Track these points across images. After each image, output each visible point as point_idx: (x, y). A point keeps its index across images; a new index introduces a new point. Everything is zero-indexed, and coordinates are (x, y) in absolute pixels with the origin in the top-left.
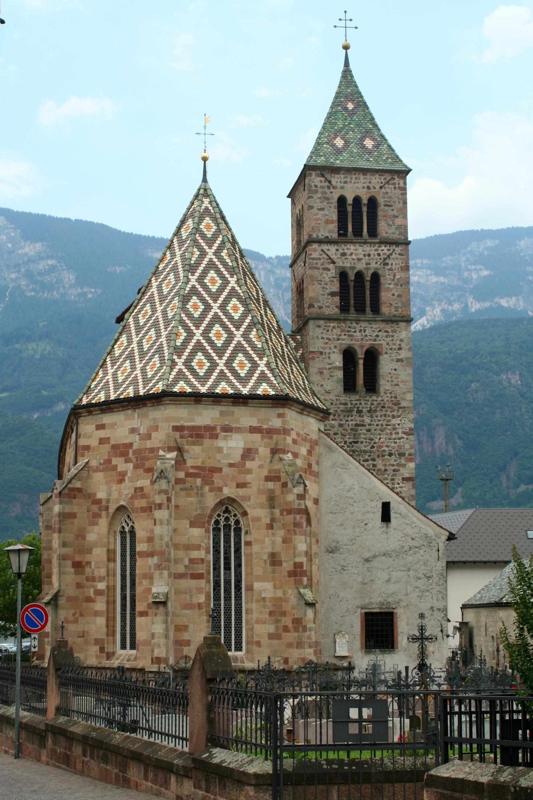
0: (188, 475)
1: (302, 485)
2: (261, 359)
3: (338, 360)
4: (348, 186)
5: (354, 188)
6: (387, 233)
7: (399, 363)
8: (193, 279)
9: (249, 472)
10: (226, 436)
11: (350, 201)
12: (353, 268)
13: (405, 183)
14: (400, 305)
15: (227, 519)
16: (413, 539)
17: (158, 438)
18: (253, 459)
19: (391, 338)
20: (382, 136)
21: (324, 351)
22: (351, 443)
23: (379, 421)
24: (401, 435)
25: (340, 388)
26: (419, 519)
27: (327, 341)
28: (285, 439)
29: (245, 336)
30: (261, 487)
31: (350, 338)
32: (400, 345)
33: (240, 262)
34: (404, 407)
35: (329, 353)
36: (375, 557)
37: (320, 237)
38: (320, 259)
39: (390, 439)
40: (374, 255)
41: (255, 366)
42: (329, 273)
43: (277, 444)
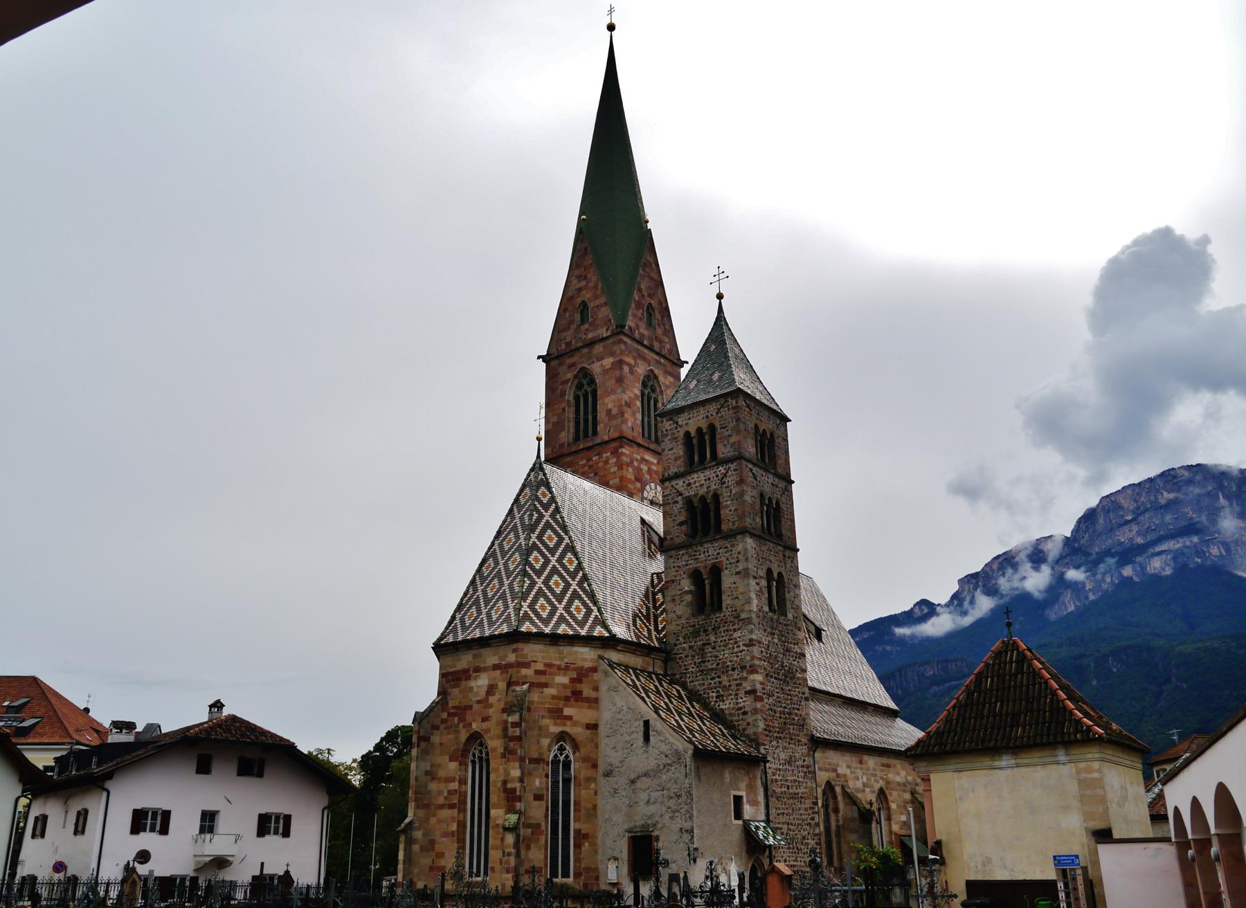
0: (450, 715)
3: (686, 585)
9: (491, 706)
12: (696, 495)
15: (481, 752)
24: (742, 648)
36: (638, 778)
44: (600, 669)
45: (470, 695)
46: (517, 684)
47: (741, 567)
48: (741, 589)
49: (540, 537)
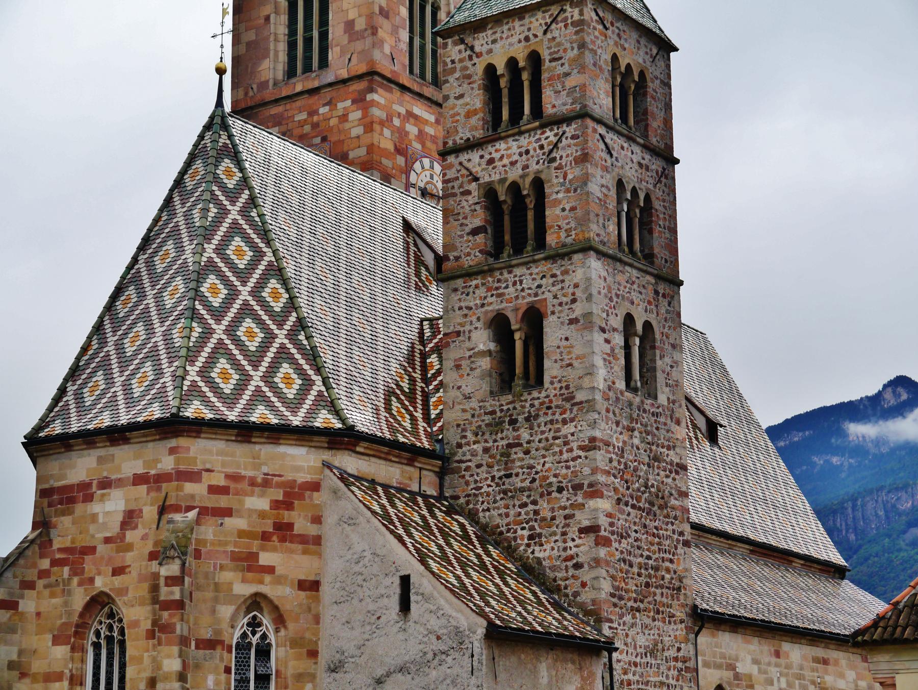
0: (54, 563)
1: (178, 562)
3: (482, 340)
4: (497, 47)
6: (554, 106)
7: (572, 326)
9: (129, 547)
10: (103, 495)
11: (500, 70)
12: (502, 181)
15: (110, 628)
16: (438, 638)
18: (136, 527)
19: (560, 286)
21: (462, 329)
22: (500, 478)
23: (543, 433)
24: (577, 452)
26: (447, 601)
27: (465, 311)
30: (143, 572)
31: (499, 300)
32: (573, 294)
34: (581, 403)
35: (470, 331)
36: (388, 675)
37: (458, 142)
38: (457, 178)
39: (559, 462)
40: (535, 150)
42: (469, 198)
45: (92, 528)
46: (177, 509)
47: (579, 310)
48: (578, 350)
49: (220, 250)
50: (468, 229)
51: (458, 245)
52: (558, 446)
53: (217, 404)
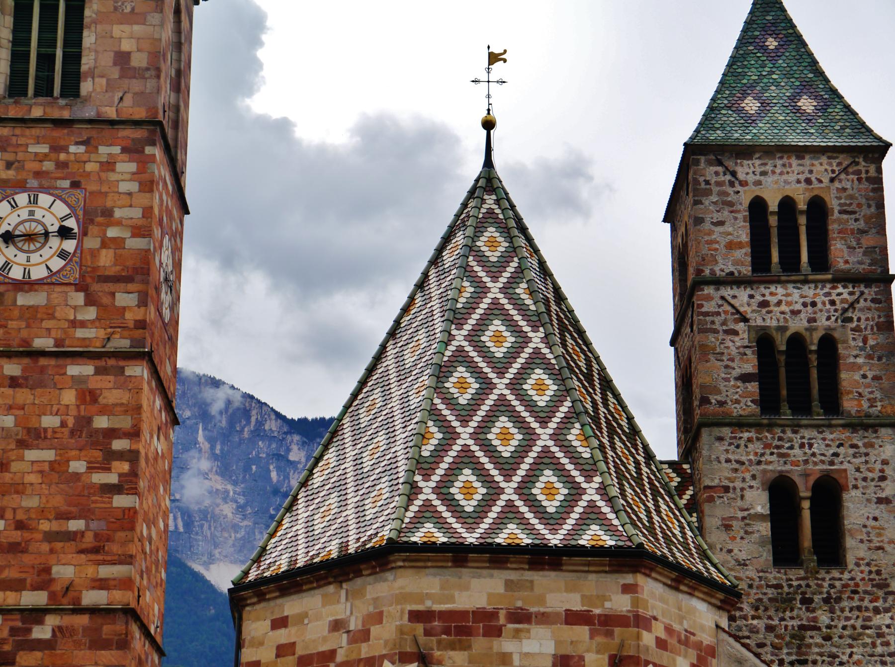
2: (589, 479)
3: (759, 502)
4: (769, 180)
5: (778, 183)
6: (847, 262)
7: (882, 506)
8: (460, 337)
10: (518, 631)
11: (773, 206)
12: (782, 329)
13: (879, 170)
14: (878, 395)
17: (383, 636)
19: (863, 459)
20: (834, 92)
21: (731, 485)
23: (848, 619)
25: (766, 555)
28: (638, 637)
29: (558, 436)
31: (782, 460)
32: (882, 471)
33: (554, 307)
35: (742, 489)
37: (718, 273)
38: (718, 314)
39: (872, 655)
40: (824, 303)
41: (576, 492)
42: (736, 339)
43: (622, 646)
44: (720, 650)
49: (474, 337)
50: (737, 372)
51: (723, 389)
52: (869, 636)
53: (455, 526)
